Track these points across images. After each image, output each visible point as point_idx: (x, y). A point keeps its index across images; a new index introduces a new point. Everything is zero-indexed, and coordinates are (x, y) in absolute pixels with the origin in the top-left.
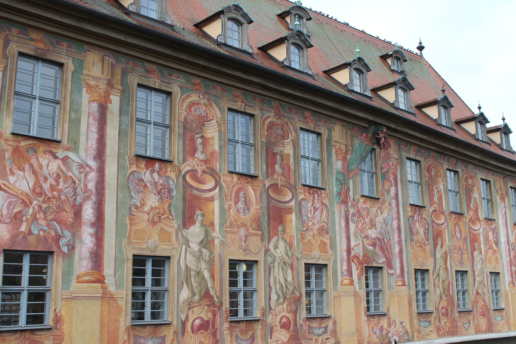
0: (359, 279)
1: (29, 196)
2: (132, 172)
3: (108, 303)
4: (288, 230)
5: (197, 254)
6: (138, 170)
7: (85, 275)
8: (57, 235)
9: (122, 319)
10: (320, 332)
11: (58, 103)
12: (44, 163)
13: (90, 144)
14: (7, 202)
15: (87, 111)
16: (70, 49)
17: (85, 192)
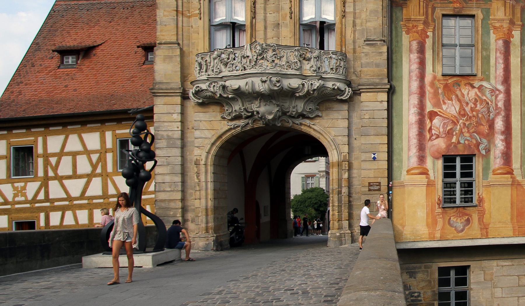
3: (517, 188)
7: (498, 169)
11: (473, 46)
12: (465, 92)
13: (498, 73)
15: (495, 48)
16: (478, 2)
17: (496, 110)
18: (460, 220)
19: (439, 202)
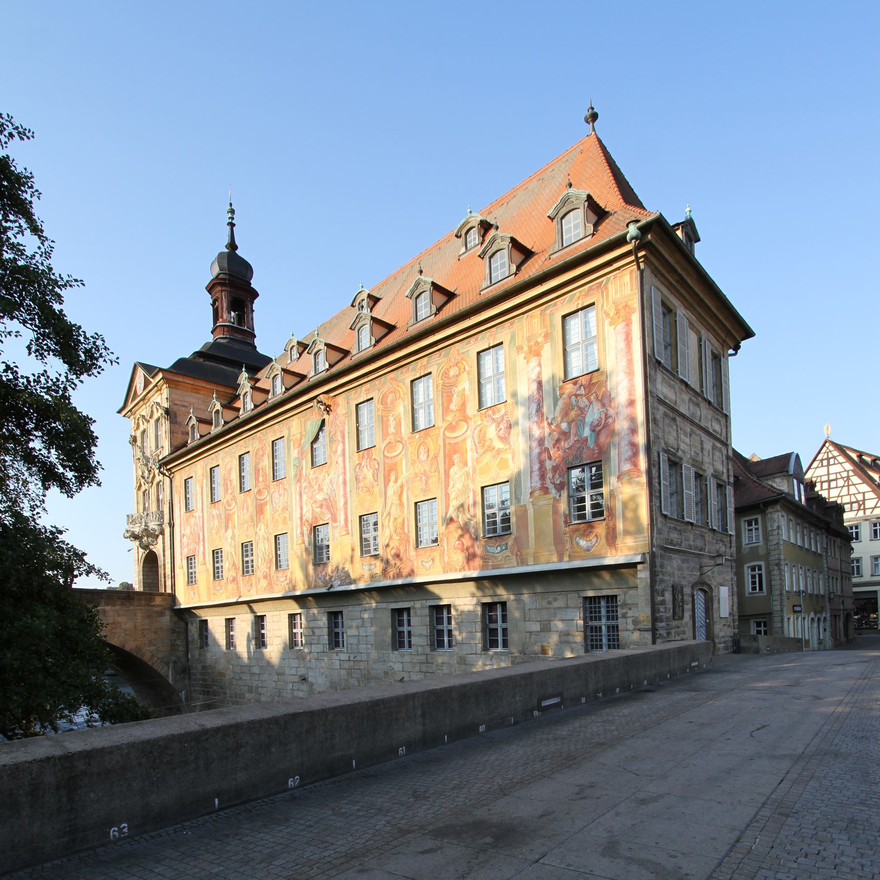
10: (283, 579)
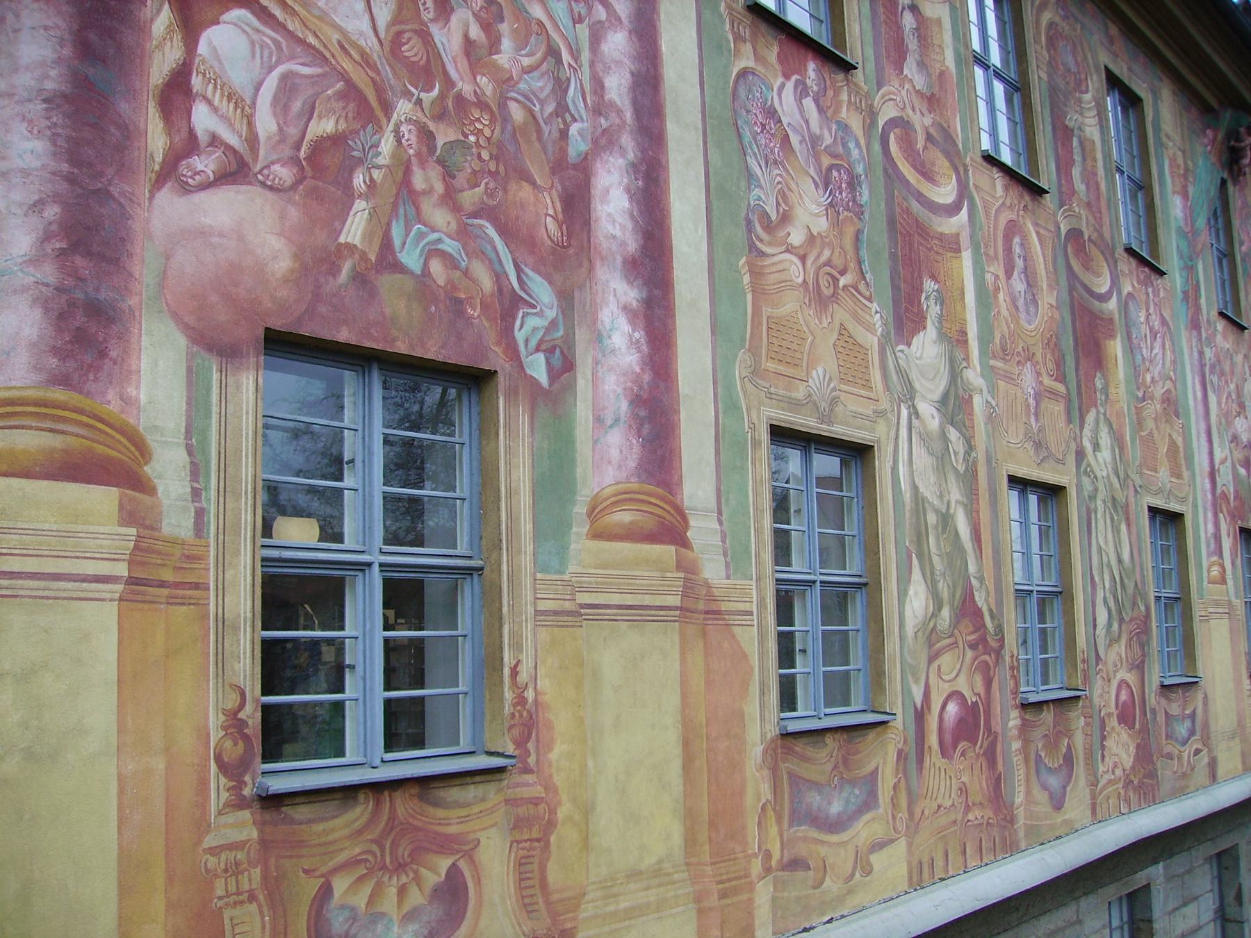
0: (1233, 564)
1: (378, 72)
2: (744, 73)
3: (704, 634)
4: (1112, 390)
5: (937, 446)
6: (760, 69)
8: (500, 291)
9: (752, 708)
14: (276, 74)
18: (402, 891)
19: (233, 750)
